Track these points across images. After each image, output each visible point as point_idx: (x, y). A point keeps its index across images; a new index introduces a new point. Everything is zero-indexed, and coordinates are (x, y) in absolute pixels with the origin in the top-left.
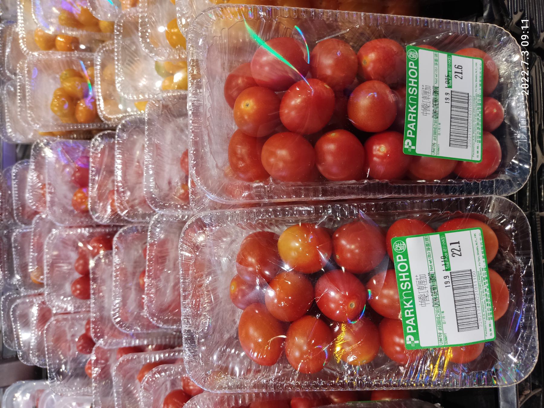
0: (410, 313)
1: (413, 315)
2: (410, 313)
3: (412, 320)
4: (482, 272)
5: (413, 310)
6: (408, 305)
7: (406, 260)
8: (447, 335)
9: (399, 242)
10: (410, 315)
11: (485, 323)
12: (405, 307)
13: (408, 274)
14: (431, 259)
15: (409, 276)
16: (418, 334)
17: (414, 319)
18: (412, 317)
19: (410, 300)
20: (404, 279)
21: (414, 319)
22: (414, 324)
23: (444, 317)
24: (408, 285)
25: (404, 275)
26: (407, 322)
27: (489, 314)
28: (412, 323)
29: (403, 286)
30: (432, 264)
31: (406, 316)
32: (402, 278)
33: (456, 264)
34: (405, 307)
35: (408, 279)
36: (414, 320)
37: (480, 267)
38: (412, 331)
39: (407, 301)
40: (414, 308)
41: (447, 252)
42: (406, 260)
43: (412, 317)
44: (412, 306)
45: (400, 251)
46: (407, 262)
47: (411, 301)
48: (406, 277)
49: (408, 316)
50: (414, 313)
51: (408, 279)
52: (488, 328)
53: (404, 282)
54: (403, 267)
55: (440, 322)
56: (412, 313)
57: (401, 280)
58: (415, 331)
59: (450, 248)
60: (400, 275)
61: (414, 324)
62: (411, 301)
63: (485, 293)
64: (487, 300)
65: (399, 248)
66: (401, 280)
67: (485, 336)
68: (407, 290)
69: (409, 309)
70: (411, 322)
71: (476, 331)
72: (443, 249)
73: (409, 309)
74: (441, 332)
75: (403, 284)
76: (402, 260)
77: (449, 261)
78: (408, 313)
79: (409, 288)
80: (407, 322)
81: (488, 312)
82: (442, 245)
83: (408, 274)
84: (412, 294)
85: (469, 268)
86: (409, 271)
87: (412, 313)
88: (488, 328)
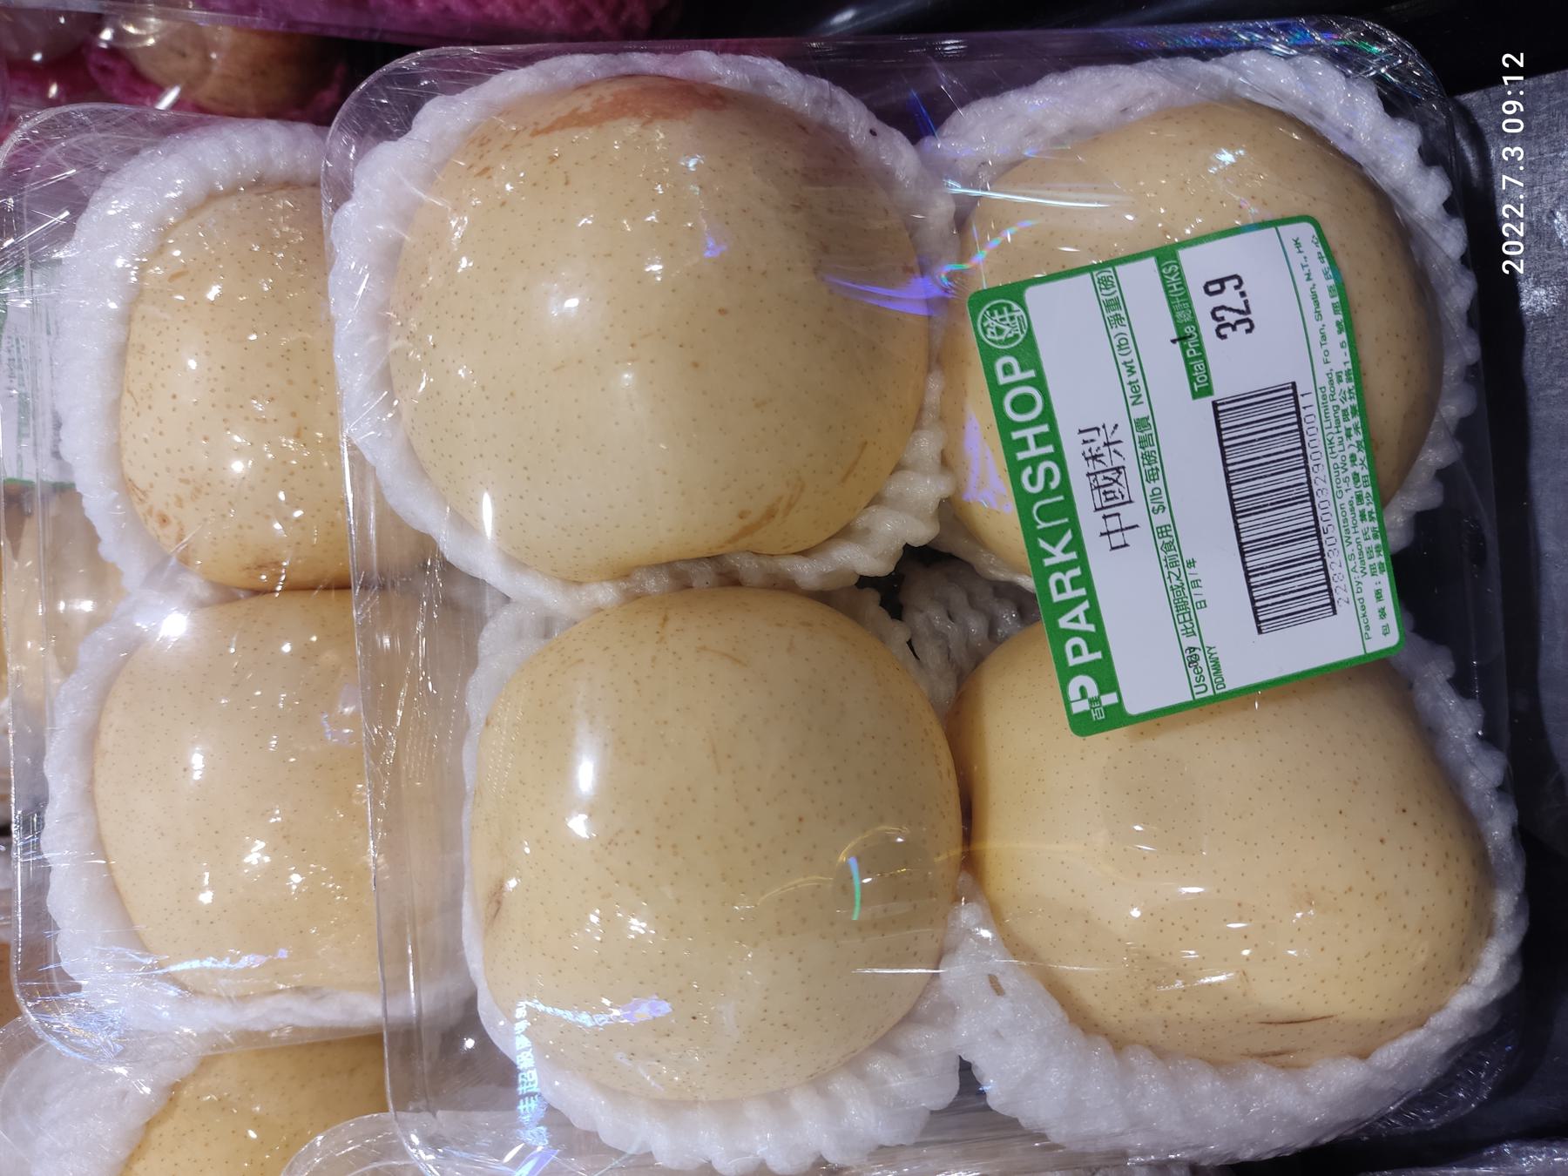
0: (1068, 586)
1: (1082, 592)
2: (1068, 586)
3: (1079, 611)
4: (1338, 387)
5: (1077, 572)
6: (1058, 555)
7: (1031, 374)
8: (1220, 653)
9: (999, 308)
10: (1070, 594)
11: (1356, 588)
12: (1048, 562)
13: (1045, 428)
14: (1133, 355)
15: (1052, 437)
16: (1110, 659)
17: (1086, 605)
18: (1077, 602)
19: (1061, 531)
20: (1034, 451)
21: (1086, 605)
22: (1092, 628)
23: (1196, 584)
24: (1049, 474)
25: (1028, 434)
26: (1064, 623)
27: (1369, 550)
28: (1083, 626)
30: (1138, 376)
31: (1056, 597)
32: (1027, 448)
33: (1238, 366)
34: (1048, 562)
35: (1050, 449)
36: (1086, 612)
37: (1327, 368)
38: (1087, 657)
39: (1053, 536)
40: (1082, 561)
41: (1194, 322)
42: (1031, 374)
43: (1077, 602)
44: (1073, 555)
45: (1008, 341)
46: (1040, 382)
47: (1068, 536)
48: (1040, 440)
49: (1063, 597)
50: (1085, 580)
51: (1050, 449)
52: (1372, 607)
53: (1034, 462)
54: (1023, 404)
55: (1184, 605)
56: (1075, 583)
57: (1021, 456)
58: (1098, 655)
59: (1203, 305)
60: (1016, 435)
61: (1092, 628)
62: (1068, 536)
63: (1351, 470)
64: (1359, 498)
65: (1000, 331)
66: (1021, 456)
67: (1364, 637)
68: (1046, 493)
69: (1063, 567)
70: (1076, 620)
71: (1327, 624)
72: (1173, 312)
73: (1063, 567)
74: (1194, 641)
75: (1028, 471)
76: (1018, 375)
77: (1203, 357)
78: (1060, 587)
79: (1054, 485)
80: (1064, 623)
81: (1365, 544)
82: (1169, 299)
83: (1045, 428)
84: (1067, 507)
85: (1287, 379)
86: (1048, 416)
87: (1075, 583)
88: (1372, 607)
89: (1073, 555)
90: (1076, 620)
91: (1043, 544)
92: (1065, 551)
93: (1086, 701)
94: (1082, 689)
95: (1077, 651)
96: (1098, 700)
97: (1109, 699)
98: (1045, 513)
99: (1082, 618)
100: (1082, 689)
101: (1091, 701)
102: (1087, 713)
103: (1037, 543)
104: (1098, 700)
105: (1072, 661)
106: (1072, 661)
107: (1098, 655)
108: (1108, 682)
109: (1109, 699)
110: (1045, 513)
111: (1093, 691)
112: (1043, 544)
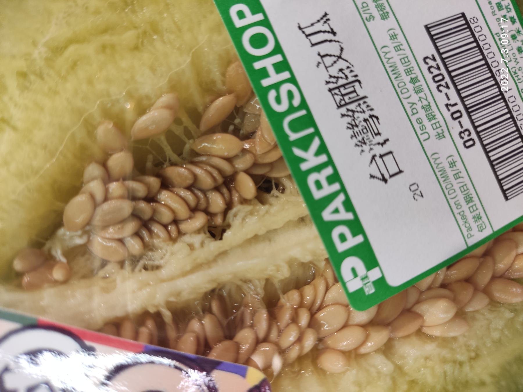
0: (324, 183)
1: (336, 187)
2: (324, 183)
3: (338, 202)
5: (329, 171)
10: (328, 189)
12: (304, 167)
17: (341, 197)
20: (274, 78)
21: (341, 197)
22: (350, 216)
24: (290, 95)
29: (278, 100)
31: (318, 195)
34: (304, 167)
53: (276, 86)
54: (259, 41)
57: (265, 83)
58: (360, 239)
60: (258, 65)
61: (350, 216)
66: (265, 83)
68: (292, 109)
69: (318, 169)
70: (336, 211)
73: (318, 169)
79: (296, 102)
89: (323, 158)
90: (336, 211)
91: (298, 152)
92: (318, 153)
93: (358, 279)
94: (353, 270)
95: (343, 238)
96: (366, 277)
97: (375, 274)
98: (295, 126)
99: (342, 209)
100: (353, 270)
101: (363, 279)
102: (361, 290)
103: (292, 152)
104: (366, 277)
105: (341, 247)
106: (341, 247)
107: (360, 239)
108: (371, 262)
109: (375, 274)
110: (295, 126)
111: (361, 268)
112: (298, 152)
